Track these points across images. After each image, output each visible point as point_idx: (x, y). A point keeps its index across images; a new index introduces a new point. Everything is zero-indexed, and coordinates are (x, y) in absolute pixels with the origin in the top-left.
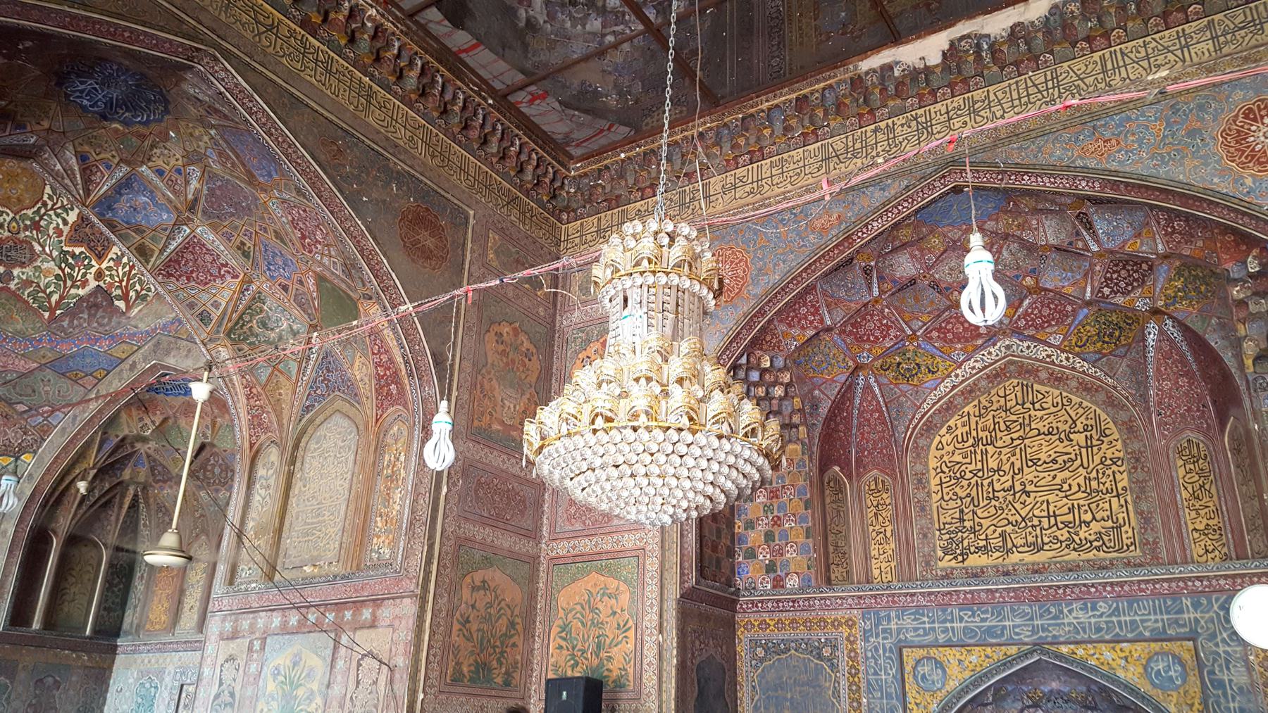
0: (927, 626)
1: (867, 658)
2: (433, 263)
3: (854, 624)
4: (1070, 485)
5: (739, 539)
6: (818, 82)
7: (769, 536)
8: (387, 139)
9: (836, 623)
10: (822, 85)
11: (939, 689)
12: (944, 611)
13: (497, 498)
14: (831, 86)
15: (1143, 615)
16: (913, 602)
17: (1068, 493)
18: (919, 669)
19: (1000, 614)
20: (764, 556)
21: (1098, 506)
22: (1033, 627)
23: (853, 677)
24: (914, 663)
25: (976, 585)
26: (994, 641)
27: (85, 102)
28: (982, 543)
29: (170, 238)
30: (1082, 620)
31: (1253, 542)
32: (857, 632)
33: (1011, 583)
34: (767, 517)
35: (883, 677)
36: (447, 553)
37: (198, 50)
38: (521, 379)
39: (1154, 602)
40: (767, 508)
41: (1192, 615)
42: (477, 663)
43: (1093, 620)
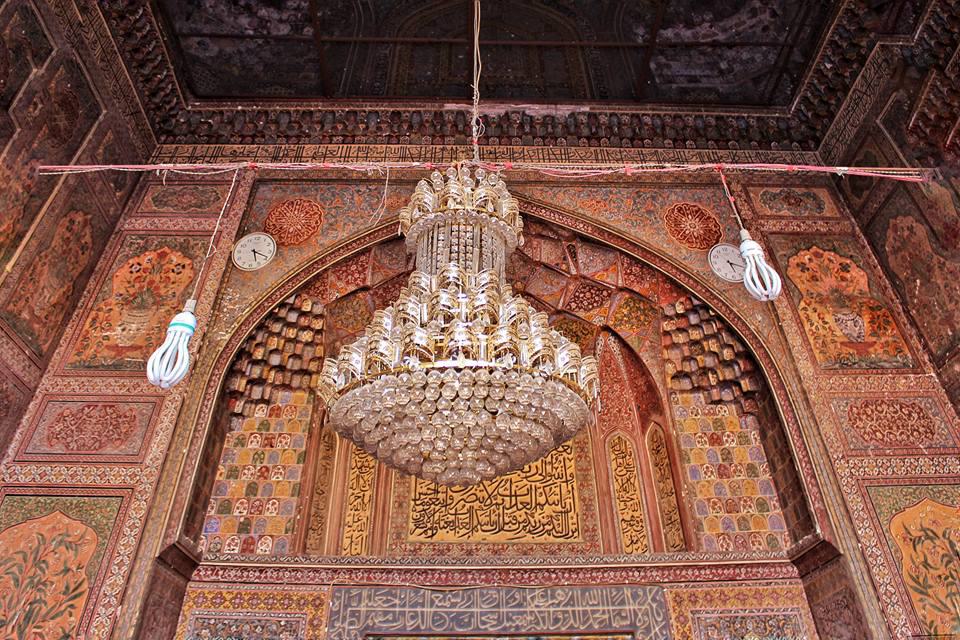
0: (397, 609)
4: (530, 467)
5: (218, 489)
6: (412, 106)
7: (252, 489)
9: (302, 601)
10: (414, 109)
12: (417, 593)
14: (419, 112)
15: (593, 605)
16: (387, 580)
17: (528, 474)
19: (469, 599)
20: (240, 512)
21: (551, 489)
25: (454, 564)
26: (460, 630)
28: (452, 518)
30: (542, 609)
31: (668, 536)
32: (324, 613)
33: (484, 564)
34: (255, 467)
39: (602, 592)
40: (258, 456)
41: (630, 607)
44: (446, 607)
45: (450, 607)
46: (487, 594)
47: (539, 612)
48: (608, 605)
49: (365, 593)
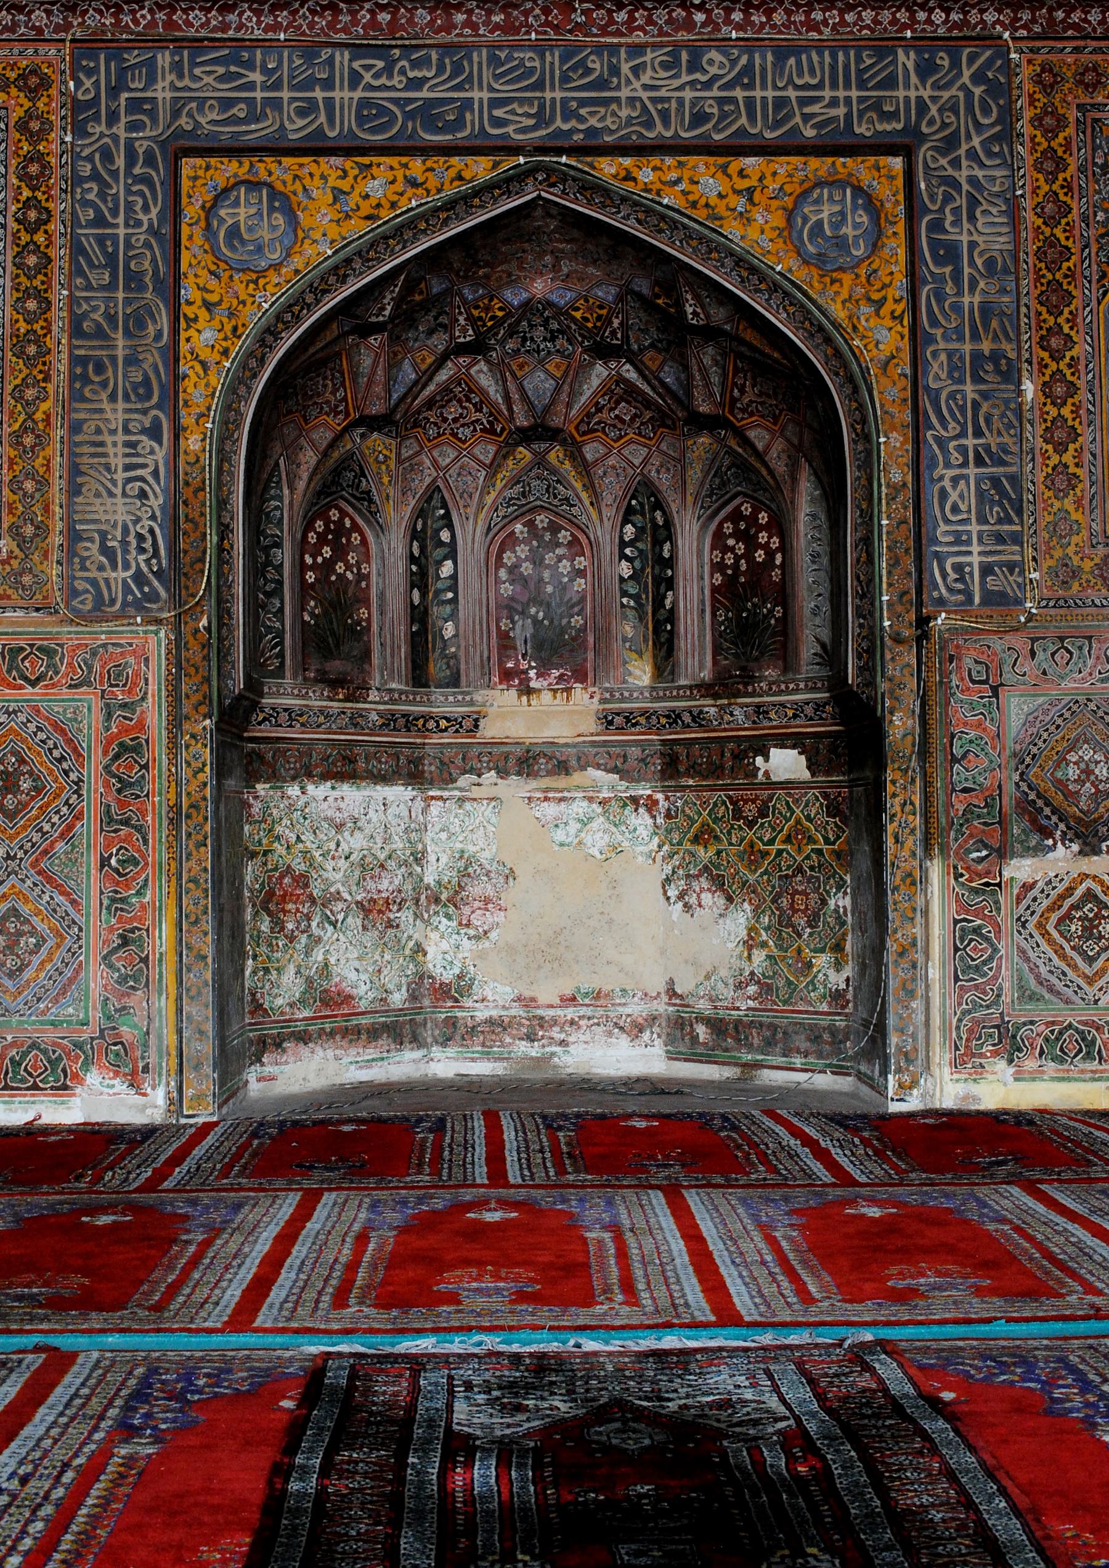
0: (259, 95)
1: (77, 180)
3: (45, 83)
11: (276, 267)
18: (223, 213)
19: (458, 69)
22: (542, 107)
23: (32, 231)
24: (209, 197)
30: (663, 93)
35: (121, 231)
43: (688, 94)
44: (393, 88)
45: (406, 89)
46: (510, 58)
47: (654, 100)
48: (847, 86)
49: (164, 59)
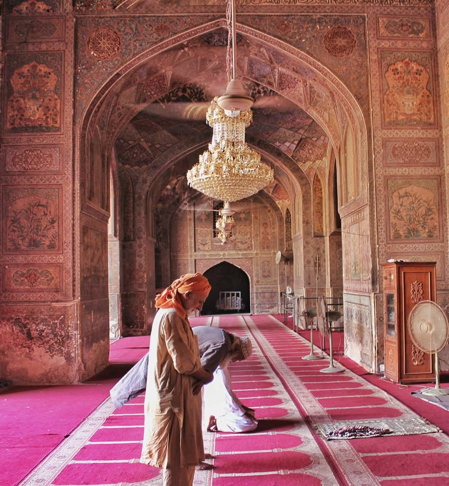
2: (347, 52)
8: (308, 7)
13: (408, 152)
27: (221, 44)
29: (274, 76)
36: (380, 184)
37: (218, 22)
38: (414, 87)
42: (409, 229)
